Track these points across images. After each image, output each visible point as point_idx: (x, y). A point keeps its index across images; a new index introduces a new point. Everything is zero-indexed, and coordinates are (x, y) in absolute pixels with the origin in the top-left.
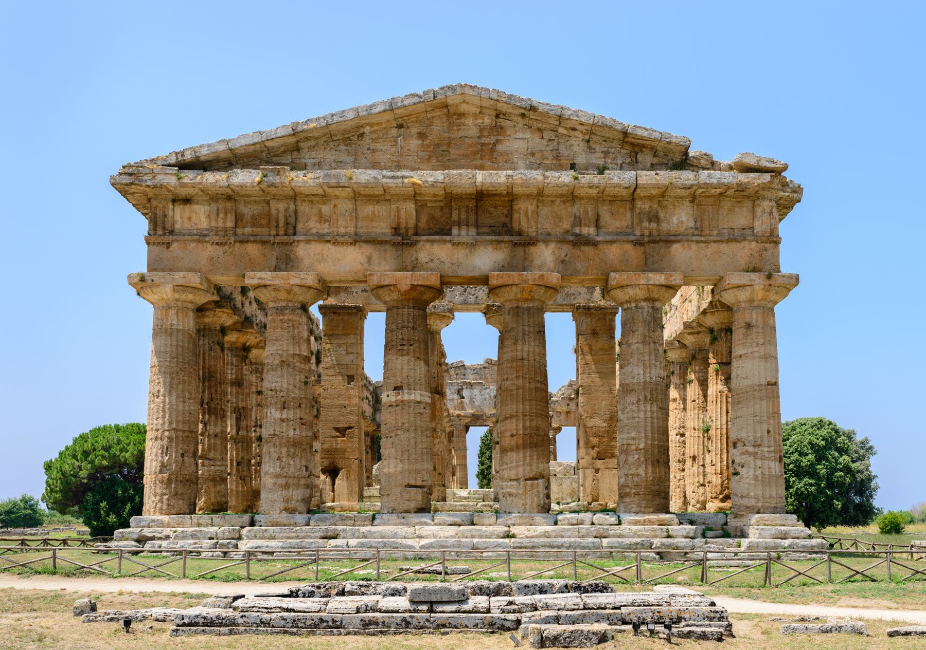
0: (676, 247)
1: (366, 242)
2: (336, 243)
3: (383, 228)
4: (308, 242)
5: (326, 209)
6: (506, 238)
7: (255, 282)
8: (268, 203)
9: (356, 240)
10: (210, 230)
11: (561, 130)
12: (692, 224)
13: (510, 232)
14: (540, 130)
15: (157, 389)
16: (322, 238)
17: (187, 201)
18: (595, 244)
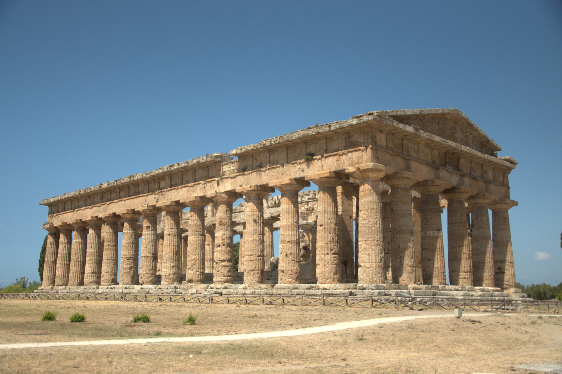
0: (492, 185)
1: (428, 165)
2: (421, 163)
3: (429, 159)
4: (414, 160)
5: (416, 147)
6: (459, 173)
7: (408, 176)
8: (403, 140)
9: (427, 164)
10: (387, 147)
11: (468, 133)
12: (492, 177)
13: (458, 170)
14: (463, 132)
15: (376, 220)
16: (417, 160)
17: (381, 131)
18: (476, 180)
